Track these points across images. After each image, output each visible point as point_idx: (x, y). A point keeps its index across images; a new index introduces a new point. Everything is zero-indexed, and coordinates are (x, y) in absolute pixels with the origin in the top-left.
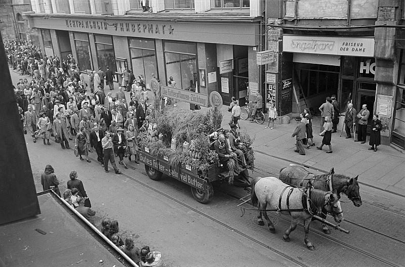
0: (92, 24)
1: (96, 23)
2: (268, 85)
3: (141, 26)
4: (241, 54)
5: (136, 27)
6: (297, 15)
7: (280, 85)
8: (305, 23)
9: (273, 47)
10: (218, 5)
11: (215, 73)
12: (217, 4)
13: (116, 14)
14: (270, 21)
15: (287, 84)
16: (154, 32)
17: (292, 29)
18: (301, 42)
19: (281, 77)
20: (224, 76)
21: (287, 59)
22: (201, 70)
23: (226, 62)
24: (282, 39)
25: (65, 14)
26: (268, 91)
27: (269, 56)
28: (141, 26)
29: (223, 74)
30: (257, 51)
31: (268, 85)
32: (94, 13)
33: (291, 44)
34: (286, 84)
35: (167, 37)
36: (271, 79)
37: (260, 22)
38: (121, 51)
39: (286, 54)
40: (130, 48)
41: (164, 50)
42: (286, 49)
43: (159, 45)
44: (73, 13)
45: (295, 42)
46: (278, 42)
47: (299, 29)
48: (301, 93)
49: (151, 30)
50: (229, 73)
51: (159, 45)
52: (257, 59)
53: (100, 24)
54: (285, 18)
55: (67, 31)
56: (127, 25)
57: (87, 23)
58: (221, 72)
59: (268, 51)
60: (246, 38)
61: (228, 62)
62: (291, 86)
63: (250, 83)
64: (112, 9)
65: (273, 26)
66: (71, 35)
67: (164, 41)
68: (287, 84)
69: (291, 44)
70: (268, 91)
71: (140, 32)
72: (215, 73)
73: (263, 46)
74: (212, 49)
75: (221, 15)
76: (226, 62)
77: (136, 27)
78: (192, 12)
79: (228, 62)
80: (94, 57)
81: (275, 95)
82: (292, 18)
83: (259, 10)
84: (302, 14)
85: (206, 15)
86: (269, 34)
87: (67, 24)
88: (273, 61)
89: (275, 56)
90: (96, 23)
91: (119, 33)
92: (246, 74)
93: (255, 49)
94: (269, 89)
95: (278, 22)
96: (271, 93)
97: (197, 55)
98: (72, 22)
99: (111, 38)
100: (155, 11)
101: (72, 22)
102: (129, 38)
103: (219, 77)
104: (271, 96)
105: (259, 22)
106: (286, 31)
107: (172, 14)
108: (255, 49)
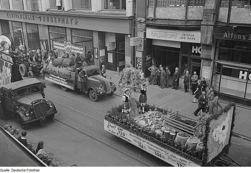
0: (24, 16)
1: (27, 16)
2: (137, 58)
3: (57, 19)
4: (121, 39)
5: (54, 20)
6: (155, 16)
7: (144, 59)
8: (159, 21)
9: (140, 35)
10: (106, 7)
11: (104, 50)
12: (106, 7)
13: (40, 10)
14: (139, 19)
15: (149, 58)
16: (65, 23)
17: (152, 24)
18: (158, 33)
19: (145, 54)
20: (110, 52)
21: (149, 43)
22: (95, 48)
23: (111, 43)
24: (146, 30)
25: (6, 9)
26: (137, 62)
27: (138, 41)
28: (57, 19)
29: (109, 51)
30: (130, 37)
31: (137, 58)
32: (26, 9)
33: (151, 34)
34: (148, 58)
35: (74, 26)
36: (139, 55)
37: (132, 19)
38: (44, 34)
39: (148, 39)
40: (49, 33)
41: (71, 34)
42: (148, 36)
43: (68, 32)
44: (11, 9)
45: (154, 33)
46: (143, 33)
47: (156, 25)
48: (157, 64)
49: (63, 21)
50: (113, 50)
51: (68, 32)
52: (131, 42)
53: (30, 17)
54: (147, 18)
55: (8, 20)
56: (48, 18)
57: (21, 16)
58: (108, 50)
59: (137, 37)
60: (124, 29)
61: (112, 43)
62: (151, 59)
63: (126, 57)
64: (38, 7)
65: (140, 22)
66: (10, 23)
67: (71, 29)
68: (149, 58)
69: (151, 34)
70: (137, 62)
71: (56, 22)
72: (104, 50)
73: (134, 34)
74: (102, 35)
75: (108, 14)
76: (111, 43)
77: (54, 20)
78: (90, 11)
79: (112, 43)
80: (26, 39)
81: (141, 65)
82: (152, 18)
83: (132, 12)
84: (158, 16)
85: (99, 13)
86: (138, 27)
87: (8, 15)
88: (140, 44)
89: (141, 41)
90: (27, 16)
91: (42, 23)
92: (124, 51)
93: (129, 36)
94: (138, 61)
95: (143, 20)
96: (139, 63)
97: (93, 38)
98: (11, 15)
99: (37, 26)
100: (66, 9)
101: (11, 15)
102: (49, 26)
103: (107, 52)
104: (139, 65)
105: (132, 20)
106: (148, 26)
107: (77, 12)
108: (129, 36)
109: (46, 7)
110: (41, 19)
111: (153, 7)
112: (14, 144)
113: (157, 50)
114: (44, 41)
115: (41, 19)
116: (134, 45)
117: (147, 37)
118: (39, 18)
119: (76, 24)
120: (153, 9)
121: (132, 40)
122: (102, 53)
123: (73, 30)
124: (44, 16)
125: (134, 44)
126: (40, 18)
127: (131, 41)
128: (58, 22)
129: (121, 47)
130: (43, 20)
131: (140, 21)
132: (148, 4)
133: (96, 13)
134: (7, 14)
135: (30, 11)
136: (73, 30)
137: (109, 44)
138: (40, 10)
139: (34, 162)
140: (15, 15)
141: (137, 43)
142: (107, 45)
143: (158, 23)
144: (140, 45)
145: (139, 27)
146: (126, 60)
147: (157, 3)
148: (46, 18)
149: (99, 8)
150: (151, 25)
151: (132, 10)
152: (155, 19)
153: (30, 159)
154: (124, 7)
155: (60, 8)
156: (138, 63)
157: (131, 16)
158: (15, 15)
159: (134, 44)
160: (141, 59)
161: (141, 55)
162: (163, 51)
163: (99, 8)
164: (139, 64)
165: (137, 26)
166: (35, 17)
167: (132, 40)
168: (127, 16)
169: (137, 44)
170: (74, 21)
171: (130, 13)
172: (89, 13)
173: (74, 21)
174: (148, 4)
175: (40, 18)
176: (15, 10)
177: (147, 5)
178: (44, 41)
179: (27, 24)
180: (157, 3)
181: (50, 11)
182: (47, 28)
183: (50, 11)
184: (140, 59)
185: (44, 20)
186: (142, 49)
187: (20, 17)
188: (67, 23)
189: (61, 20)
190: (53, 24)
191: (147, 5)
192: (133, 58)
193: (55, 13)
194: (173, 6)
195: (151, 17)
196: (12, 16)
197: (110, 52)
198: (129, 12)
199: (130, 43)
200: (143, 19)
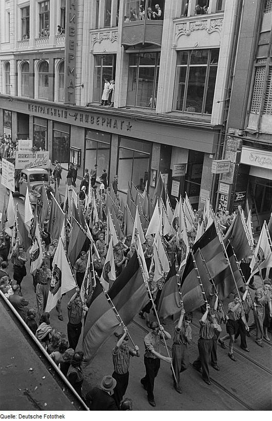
0: (53, 111)
1: (57, 111)
2: (220, 194)
3: (100, 120)
4: (197, 159)
5: (95, 120)
6: (259, 129)
7: (232, 197)
8: (266, 137)
9: (231, 157)
10: (179, 108)
11: (167, 175)
12: (179, 107)
13: (77, 104)
14: (231, 131)
15: (241, 197)
16: (112, 127)
17: (253, 142)
18: (261, 156)
19: (235, 188)
20: (176, 179)
21: (244, 171)
22: (153, 170)
23: (180, 165)
24: (241, 150)
25: (28, 98)
26: (219, 201)
27: (224, 166)
28: (100, 120)
29: (175, 177)
30: (213, 159)
31: (220, 194)
32: (56, 101)
33: (249, 156)
34: (239, 196)
35: (124, 132)
36: (224, 189)
37: (220, 131)
38: (77, 140)
39: (242, 165)
40: (85, 139)
41: (119, 145)
42: (244, 160)
43: (115, 141)
44: (36, 98)
45: (254, 156)
46: (236, 153)
47: (260, 143)
48: (253, 207)
49: (109, 123)
50: (181, 177)
51: (115, 141)
52: (213, 167)
53: (60, 113)
54: (246, 130)
56: (87, 117)
57: (48, 110)
58: (174, 175)
59: (224, 160)
60: (204, 144)
61: (181, 165)
62: (244, 199)
63: (202, 190)
64: (74, 99)
65: (233, 136)
66: (31, 121)
67: (120, 137)
68: (241, 197)
69: (249, 156)
70: (219, 201)
71: (98, 124)
72: (167, 175)
73: (220, 153)
74: (167, 151)
75: (182, 118)
76: (180, 165)
77: (95, 120)
78: (153, 112)
79: (181, 165)
80: (50, 145)
81: (226, 206)
82: (254, 130)
83: (220, 118)
84: (264, 129)
85: (166, 116)
86: (228, 144)
87: (29, 108)
88: (228, 171)
89: (231, 167)
90: (57, 111)
91: (78, 123)
92: (199, 180)
93: (211, 156)
94: (221, 199)
95: (238, 132)
96: (222, 204)
97: (151, 154)
98: (34, 107)
99: (69, 127)
100: (116, 106)
101: (34, 107)
102: (87, 130)
103: (171, 179)
104: (222, 207)
105: (219, 130)
106: (245, 143)
107: (133, 111)
108: (211, 156)
109: (87, 100)
110: (76, 118)
111: (258, 113)
112: (9, 315)
113: (257, 185)
114: (76, 151)
115: (76, 118)
116: (218, 173)
117: (242, 161)
118: (75, 116)
119: (128, 130)
120: (258, 116)
121: (215, 163)
122: (164, 178)
123: (121, 139)
124: (82, 113)
125: (219, 170)
126: (76, 116)
127: (213, 165)
128: (100, 124)
129: (195, 174)
130: (79, 120)
131: (233, 134)
132: (250, 108)
133: (162, 116)
134: (29, 105)
135: (62, 103)
136: (121, 139)
137: (178, 165)
138: (77, 104)
139: (34, 353)
140: (40, 108)
141: (223, 170)
142: (174, 167)
143: (263, 140)
144: (228, 173)
145: (231, 143)
146: (201, 195)
147: (265, 107)
148: (90, 118)
149: (167, 108)
150: (251, 143)
151: (221, 116)
152: (258, 134)
153: (32, 350)
154: (209, 110)
155: (106, 103)
156: (220, 202)
157: (219, 125)
158: (40, 108)
159: (219, 170)
160: (227, 197)
161: (228, 191)
162: (267, 187)
163: (167, 108)
164: (223, 205)
165: (226, 142)
166: (68, 114)
167: (215, 163)
168: (211, 124)
169: (224, 171)
170: (125, 125)
171: (218, 120)
172: (151, 114)
173: (125, 125)
174: (250, 108)
175: (76, 116)
176: (40, 100)
177: (248, 109)
178: (76, 151)
179: (55, 124)
180: (265, 107)
181: (91, 106)
182: (84, 132)
183: (91, 106)
184: (225, 196)
185: (81, 120)
186: (231, 180)
187: (46, 112)
188: (114, 127)
189: (106, 122)
190: (94, 127)
191: (248, 109)
192: (214, 193)
193: (99, 111)
194: (254, 113)
195: (252, 130)
196: (36, 110)
197: (176, 179)
198: (216, 118)
199: (211, 168)
200: (237, 131)
